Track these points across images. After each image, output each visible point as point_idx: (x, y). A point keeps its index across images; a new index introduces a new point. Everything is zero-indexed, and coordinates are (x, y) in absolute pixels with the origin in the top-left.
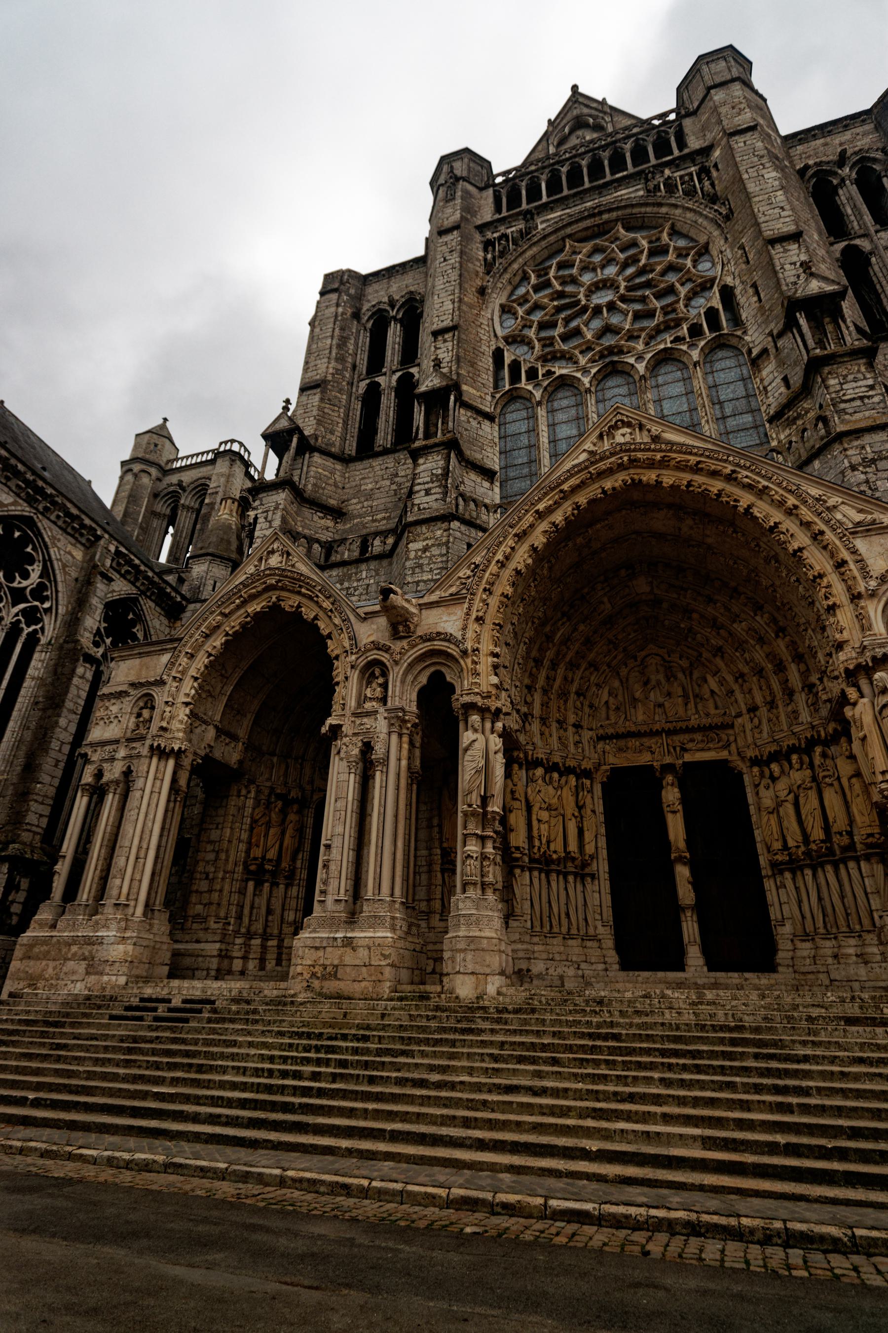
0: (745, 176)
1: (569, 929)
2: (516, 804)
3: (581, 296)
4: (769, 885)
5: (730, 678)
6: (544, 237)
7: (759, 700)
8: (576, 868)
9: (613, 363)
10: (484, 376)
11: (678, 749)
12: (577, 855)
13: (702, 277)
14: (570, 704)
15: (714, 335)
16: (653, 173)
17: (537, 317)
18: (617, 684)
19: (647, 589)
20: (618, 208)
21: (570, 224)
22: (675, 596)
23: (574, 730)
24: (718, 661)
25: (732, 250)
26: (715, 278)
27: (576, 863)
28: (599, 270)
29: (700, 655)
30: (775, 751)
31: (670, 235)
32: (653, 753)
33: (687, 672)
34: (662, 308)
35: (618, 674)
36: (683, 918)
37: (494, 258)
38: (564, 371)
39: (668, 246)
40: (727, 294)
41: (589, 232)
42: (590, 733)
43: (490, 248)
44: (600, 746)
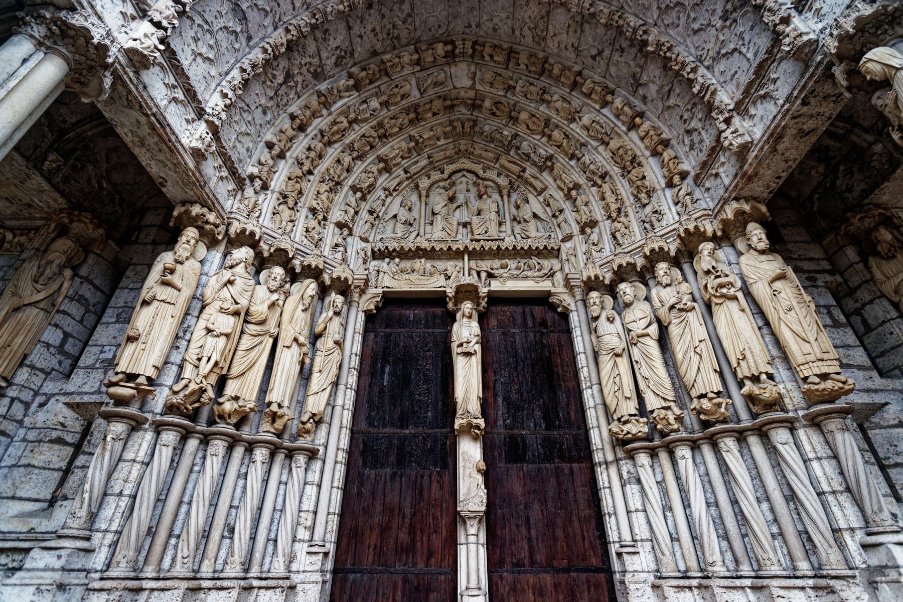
1: (226, 562)
2: (164, 293)
4: (607, 478)
5: (559, 195)
7: (598, 213)
8: (279, 435)
11: (483, 275)
12: (288, 413)
14: (339, 198)
18: (414, 198)
19: (469, 83)
22: (502, 93)
23: (337, 230)
24: (546, 177)
27: (279, 424)
29: (524, 171)
30: (628, 264)
32: (448, 278)
33: (505, 192)
35: (417, 187)
36: (461, 538)
42: (364, 245)
44: (374, 264)
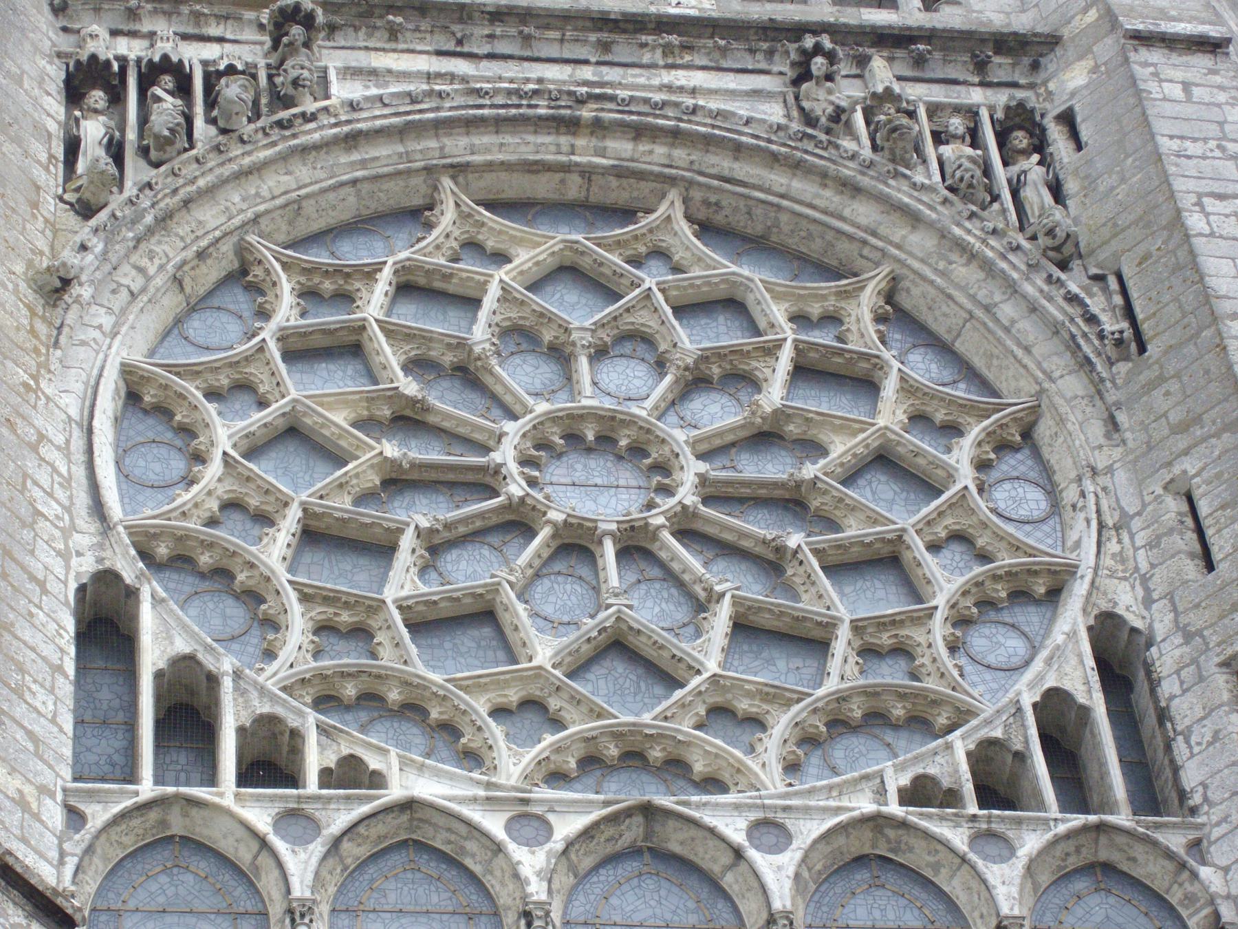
0: (1195, 222)
3: (506, 455)
6: (352, 140)
9: (648, 810)
10: (42, 700)
13: (1016, 547)
15: (1078, 820)
16: (831, 57)
17: (300, 487)
20: (675, 136)
21: (471, 124)
25: (1140, 484)
26: (1071, 571)
28: (583, 363)
31: (880, 319)
34: (858, 627)
37: (116, 150)
38: (428, 788)
39: (879, 365)
40: (1119, 658)
41: (543, 187)
43: (97, 97)
